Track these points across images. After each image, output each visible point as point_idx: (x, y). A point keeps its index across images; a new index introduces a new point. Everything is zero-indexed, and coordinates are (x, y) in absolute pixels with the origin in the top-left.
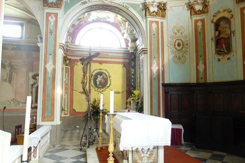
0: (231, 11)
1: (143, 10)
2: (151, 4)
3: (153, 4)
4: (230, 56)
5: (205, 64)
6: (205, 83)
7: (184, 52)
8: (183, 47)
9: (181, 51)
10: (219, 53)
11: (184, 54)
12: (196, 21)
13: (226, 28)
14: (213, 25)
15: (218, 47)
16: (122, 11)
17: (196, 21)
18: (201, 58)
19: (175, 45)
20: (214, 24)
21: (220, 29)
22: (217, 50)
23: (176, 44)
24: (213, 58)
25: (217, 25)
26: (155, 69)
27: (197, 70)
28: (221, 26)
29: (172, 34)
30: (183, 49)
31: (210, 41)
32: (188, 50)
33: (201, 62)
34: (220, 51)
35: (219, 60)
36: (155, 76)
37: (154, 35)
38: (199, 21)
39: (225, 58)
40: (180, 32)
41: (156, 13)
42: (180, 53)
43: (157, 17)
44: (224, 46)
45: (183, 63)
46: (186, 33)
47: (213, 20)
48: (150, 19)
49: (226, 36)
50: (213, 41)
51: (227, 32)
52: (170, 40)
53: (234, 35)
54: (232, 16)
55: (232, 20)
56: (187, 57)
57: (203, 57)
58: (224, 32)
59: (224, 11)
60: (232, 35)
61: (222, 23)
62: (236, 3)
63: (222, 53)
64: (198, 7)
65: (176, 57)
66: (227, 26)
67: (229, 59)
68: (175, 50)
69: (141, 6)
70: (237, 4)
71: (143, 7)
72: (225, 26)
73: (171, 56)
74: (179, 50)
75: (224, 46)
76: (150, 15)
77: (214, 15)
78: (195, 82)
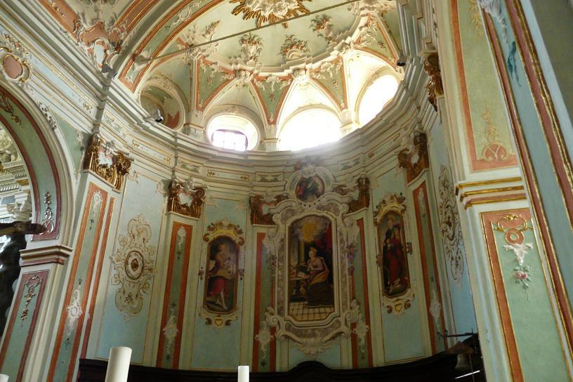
0: (240, 232)
1: (82, 149)
2: (105, 146)
3: (108, 147)
4: (230, 319)
5: (180, 326)
6: (173, 370)
7: (141, 286)
8: (141, 274)
9: (136, 281)
10: (212, 306)
11: (141, 291)
12: (177, 226)
13: (229, 259)
14: (206, 245)
15: (211, 293)
16: (28, 125)
17: (177, 226)
18: (172, 309)
19: (127, 263)
20: (209, 244)
21: (219, 257)
22: (208, 299)
23: (130, 261)
24: (197, 315)
25: (214, 248)
26: (74, 312)
27: (162, 337)
28: (221, 253)
29: (125, 234)
30: (142, 278)
31: (196, 276)
32: (150, 282)
33: (172, 318)
34: (214, 303)
35: (209, 322)
36: (69, 334)
37: (92, 221)
38: (182, 227)
39: (220, 320)
40: (143, 235)
41: (107, 170)
42: (134, 287)
43: (107, 182)
44: (222, 294)
45: (136, 311)
46: (152, 242)
47: (208, 237)
48: (92, 178)
49: (228, 276)
50: (201, 279)
51: (231, 269)
52: (118, 246)
53: (241, 279)
54: (242, 242)
55: (242, 248)
56: (146, 299)
57: (177, 308)
58: (226, 267)
60: (239, 277)
61: (224, 248)
62: (249, 221)
63: (217, 308)
64: (184, 199)
65: (124, 293)
66: (233, 256)
67: (228, 323)
68: (125, 275)
69: (80, 139)
70: (252, 224)
71: (83, 140)
72: (229, 256)
73: (114, 288)
74: (133, 278)
75: (222, 294)
76: (96, 169)
77: (209, 227)
78: (154, 365)
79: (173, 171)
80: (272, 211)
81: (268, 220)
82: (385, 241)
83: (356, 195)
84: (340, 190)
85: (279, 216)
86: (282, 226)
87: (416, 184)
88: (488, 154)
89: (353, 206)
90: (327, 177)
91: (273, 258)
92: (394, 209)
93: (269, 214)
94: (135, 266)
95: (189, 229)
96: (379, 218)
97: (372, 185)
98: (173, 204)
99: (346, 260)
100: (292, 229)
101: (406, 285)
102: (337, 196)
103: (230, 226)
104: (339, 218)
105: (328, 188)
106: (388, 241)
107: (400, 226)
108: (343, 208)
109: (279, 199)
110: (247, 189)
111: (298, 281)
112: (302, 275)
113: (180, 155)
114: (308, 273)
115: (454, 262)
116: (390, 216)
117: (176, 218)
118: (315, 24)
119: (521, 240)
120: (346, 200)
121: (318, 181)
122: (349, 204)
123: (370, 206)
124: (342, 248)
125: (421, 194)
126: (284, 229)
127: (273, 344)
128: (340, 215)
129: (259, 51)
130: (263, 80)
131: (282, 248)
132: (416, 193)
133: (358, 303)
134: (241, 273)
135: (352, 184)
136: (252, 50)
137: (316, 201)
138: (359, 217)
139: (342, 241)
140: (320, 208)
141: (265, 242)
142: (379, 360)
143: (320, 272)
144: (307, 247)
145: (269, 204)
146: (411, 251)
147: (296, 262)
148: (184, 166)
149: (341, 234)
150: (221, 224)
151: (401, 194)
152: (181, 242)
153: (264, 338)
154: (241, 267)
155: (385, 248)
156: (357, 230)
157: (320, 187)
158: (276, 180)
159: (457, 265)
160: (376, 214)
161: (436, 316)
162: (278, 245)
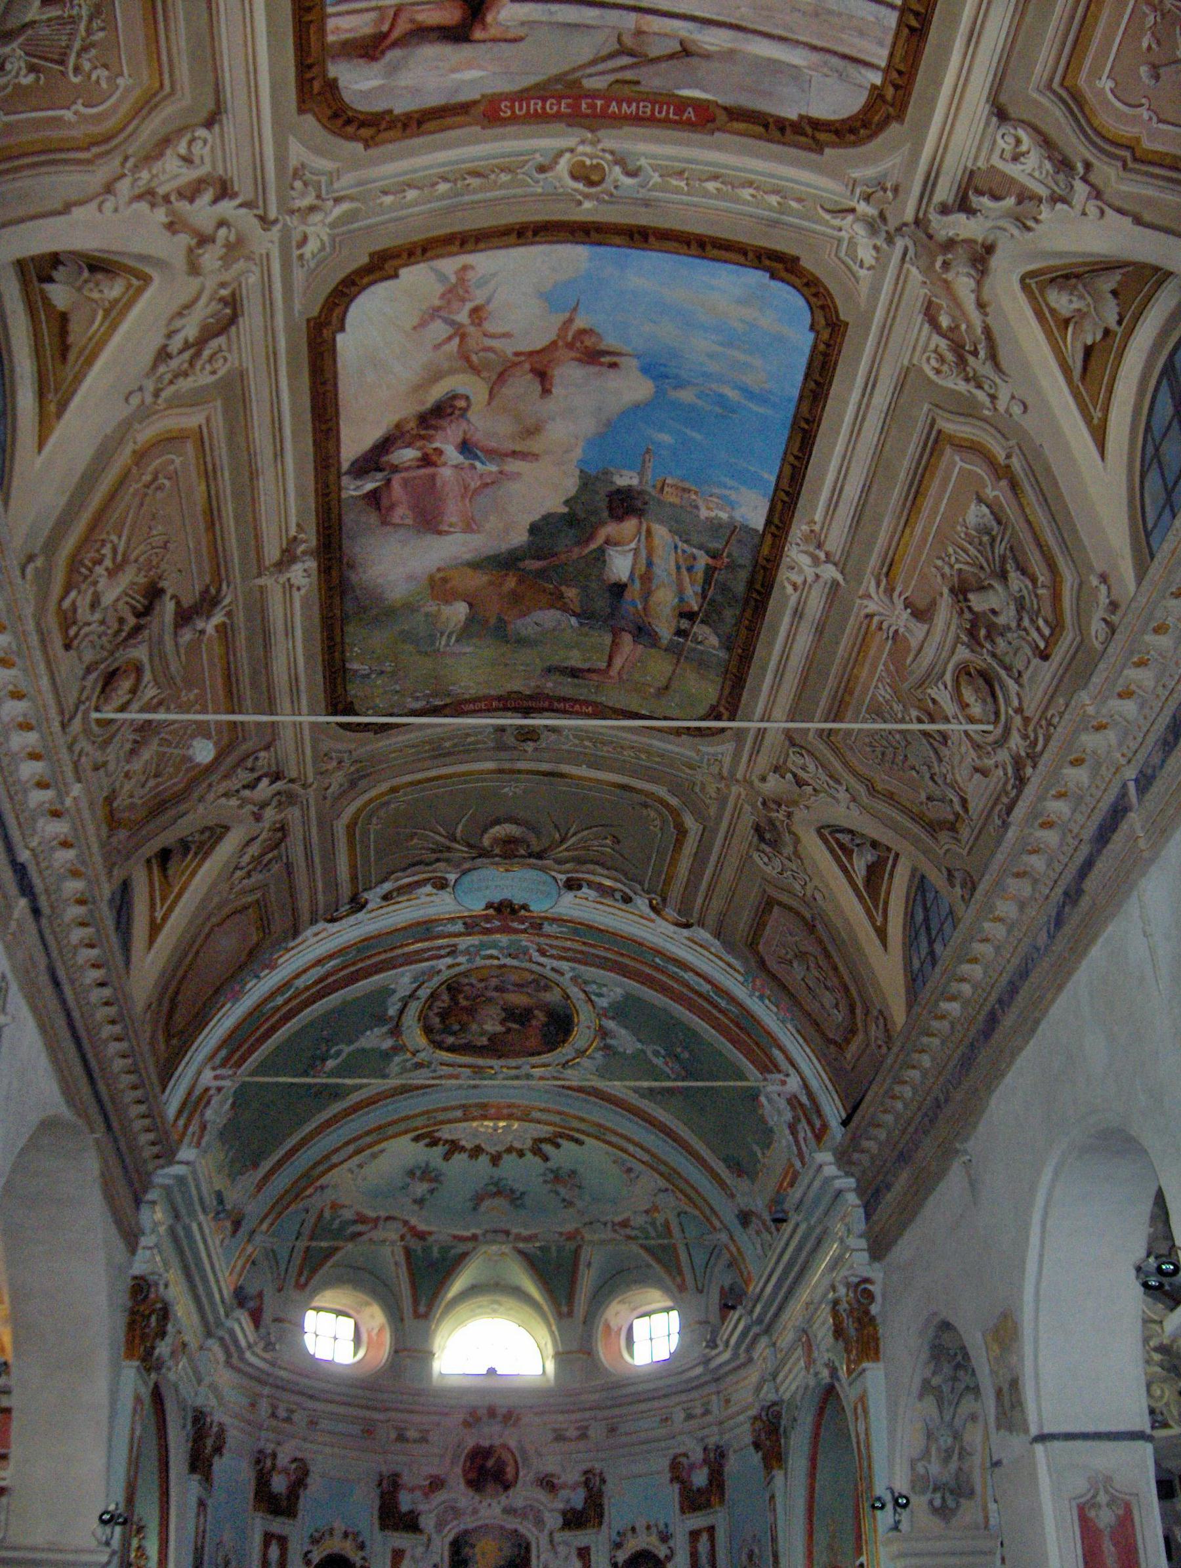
0: (362, 1547)
62: (376, 1522)
64: (279, 1484)
80: (422, 1507)
81: (410, 1524)
83: (578, 1499)
84: (548, 1484)
87: (697, 1521)
89: (574, 1520)
90: (523, 1451)
92: (651, 1548)
93: (411, 1512)
97: (609, 1489)
102: (541, 1495)
104: (544, 1540)
108: (553, 1521)
109: (436, 1484)
118: (551, 1176)
121: (506, 1456)
122: (564, 1513)
123: (604, 1527)
125: (705, 1537)
128: (546, 1532)
129: (432, 1191)
130: (421, 1236)
132: (694, 1535)
135: (572, 1476)
136: (421, 1188)
137: (503, 1498)
140: (509, 1511)
145: (412, 1490)
151: (666, 1526)
157: (510, 1470)
158: (424, 1440)
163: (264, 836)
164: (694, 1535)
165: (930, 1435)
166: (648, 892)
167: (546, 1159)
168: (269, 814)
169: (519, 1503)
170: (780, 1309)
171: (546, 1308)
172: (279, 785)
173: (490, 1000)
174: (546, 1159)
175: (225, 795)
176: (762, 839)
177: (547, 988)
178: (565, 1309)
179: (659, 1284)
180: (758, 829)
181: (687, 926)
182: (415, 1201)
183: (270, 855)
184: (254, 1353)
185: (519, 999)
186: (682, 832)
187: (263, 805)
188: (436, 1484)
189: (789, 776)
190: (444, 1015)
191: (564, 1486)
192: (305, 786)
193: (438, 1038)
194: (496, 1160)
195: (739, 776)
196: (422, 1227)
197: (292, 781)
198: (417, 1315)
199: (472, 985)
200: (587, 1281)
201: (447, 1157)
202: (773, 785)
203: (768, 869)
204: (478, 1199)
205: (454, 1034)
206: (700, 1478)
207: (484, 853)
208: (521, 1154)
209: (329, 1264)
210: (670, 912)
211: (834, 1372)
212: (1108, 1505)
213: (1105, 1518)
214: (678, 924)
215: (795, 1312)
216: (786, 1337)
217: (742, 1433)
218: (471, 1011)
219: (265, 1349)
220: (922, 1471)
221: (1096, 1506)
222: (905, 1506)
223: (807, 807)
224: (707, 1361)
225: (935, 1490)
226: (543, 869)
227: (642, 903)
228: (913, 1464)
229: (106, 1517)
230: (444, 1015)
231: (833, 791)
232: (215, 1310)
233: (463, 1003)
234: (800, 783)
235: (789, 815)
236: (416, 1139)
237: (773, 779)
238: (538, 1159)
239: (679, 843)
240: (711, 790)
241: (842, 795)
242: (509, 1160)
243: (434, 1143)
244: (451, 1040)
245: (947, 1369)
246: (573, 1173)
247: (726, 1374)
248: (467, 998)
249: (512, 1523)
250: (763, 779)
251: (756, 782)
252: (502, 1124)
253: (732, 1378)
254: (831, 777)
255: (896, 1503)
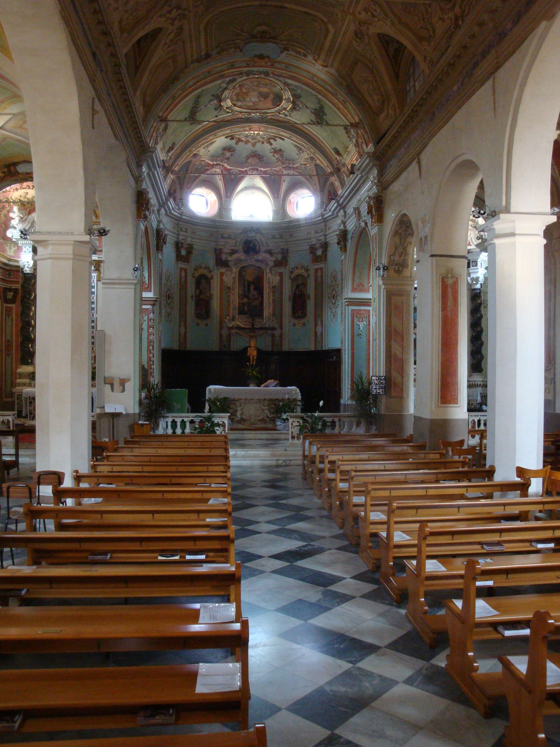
0: (210, 271)
5: (186, 328)
14: (194, 280)
17: (181, 269)
27: (180, 335)
54: (212, 278)
55: (212, 281)
59: (206, 268)
64: (183, 252)
79: (178, 235)
82: (295, 290)
83: (279, 257)
84: (270, 252)
85: (233, 262)
86: (234, 269)
88: (358, 286)
89: (278, 264)
90: (262, 242)
91: (229, 288)
94: (169, 297)
95: (186, 270)
96: (293, 276)
98: (179, 257)
99: (271, 294)
100: (240, 273)
101: (304, 315)
102: (268, 256)
103: (206, 268)
104: (268, 271)
105: (263, 249)
106: (297, 290)
107: (305, 284)
108: (271, 263)
109: (233, 252)
110: (215, 243)
111: (243, 303)
112: (245, 300)
113: (181, 223)
114: (249, 299)
115: (333, 314)
116: (300, 277)
117: (182, 265)
119: (362, 321)
120: (273, 259)
121: (257, 244)
122: (274, 262)
124: (269, 287)
125: (319, 271)
126: (235, 270)
127: (229, 336)
129: (232, 155)
131: (234, 283)
132: (316, 270)
133: (276, 318)
134: (211, 296)
136: (228, 154)
138: (280, 271)
139: (269, 283)
140: (257, 260)
141: (224, 278)
142: (286, 347)
143: (255, 299)
144: (249, 284)
146: (309, 298)
147: (242, 292)
148: (181, 230)
149: (269, 279)
150: (201, 267)
152: (183, 279)
153: (225, 332)
154: (212, 293)
155: (295, 293)
156: (278, 278)
157: (257, 248)
159: (334, 316)
160: (291, 273)
161: (319, 333)
162: (232, 281)
163: (174, 32)
164: (316, 270)
165: (396, 248)
166: (313, 54)
167: (271, 144)
168: (177, 23)
169: (260, 258)
170: (349, 201)
171: (269, 195)
172: (180, 11)
173: (253, 90)
174: (271, 144)
175: (161, 16)
176: (357, 36)
177: (275, 86)
178: (276, 196)
179: (308, 188)
180: (356, 33)
181: (326, 66)
182: (226, 159)
183: (177, 39)
184: (175, 211)
185: (265, 90)
186: (327, 31)
187: (174, 19)
188: (233, 252)
189: (369, 13)
190: (237, 95)
191: (275, 253)
192: (189, 12)
193: (235, 103)
194: (254, 145)
195: (351, 11)
196: (229, 167)
197: (184, 10)
198: (227, 196)
199: (248, 85)
200: (284, 187)
201: (237, 143)
202: (363, 16)
203: (358, 48)
204: (248, 157)
205: (241, 101)
206: (319, 252)
207: (254, 36)
208: (263, 143)
209: (197, 180)
210: (320, 62)
211: (366, 224)
212: (451, 278)
213: (450, 282)
214: (323, 66)
215: (354, 203)
216: (350, 210)
217: (333, 239)
218: (246, 94)
219: (178, 210)
220: (392, 258)
221: (447, 277)
222: (386, 270)
223: (375, 26)
224: (322, 215)
225: (396, 265)
226: (275, 43)
227: (310, 58)
228: (390, 256)
229: (135, 269)
230: (237, 95)
231: (385, 21)
232: (162, 199)
233: (244, 91)
234: (373, 16)
235: (368, 28)
236: (226, 137)
237: (363, 13)
238: (268, 145)
239: (326, 36)
240: (340, 16)
241: (388, 22)
242: (259, 145)
243: (232, 138)
244: (239, 104)
245: (404, 228)
246: (280, 150)
247: (330, 220)
248: (246, 89)
249: (258, 264)
250: (360, 13)
251: (357, 15)
252: (256, 133)
253: (331, 221)
254: (386, 15)
255: (384, 269)
